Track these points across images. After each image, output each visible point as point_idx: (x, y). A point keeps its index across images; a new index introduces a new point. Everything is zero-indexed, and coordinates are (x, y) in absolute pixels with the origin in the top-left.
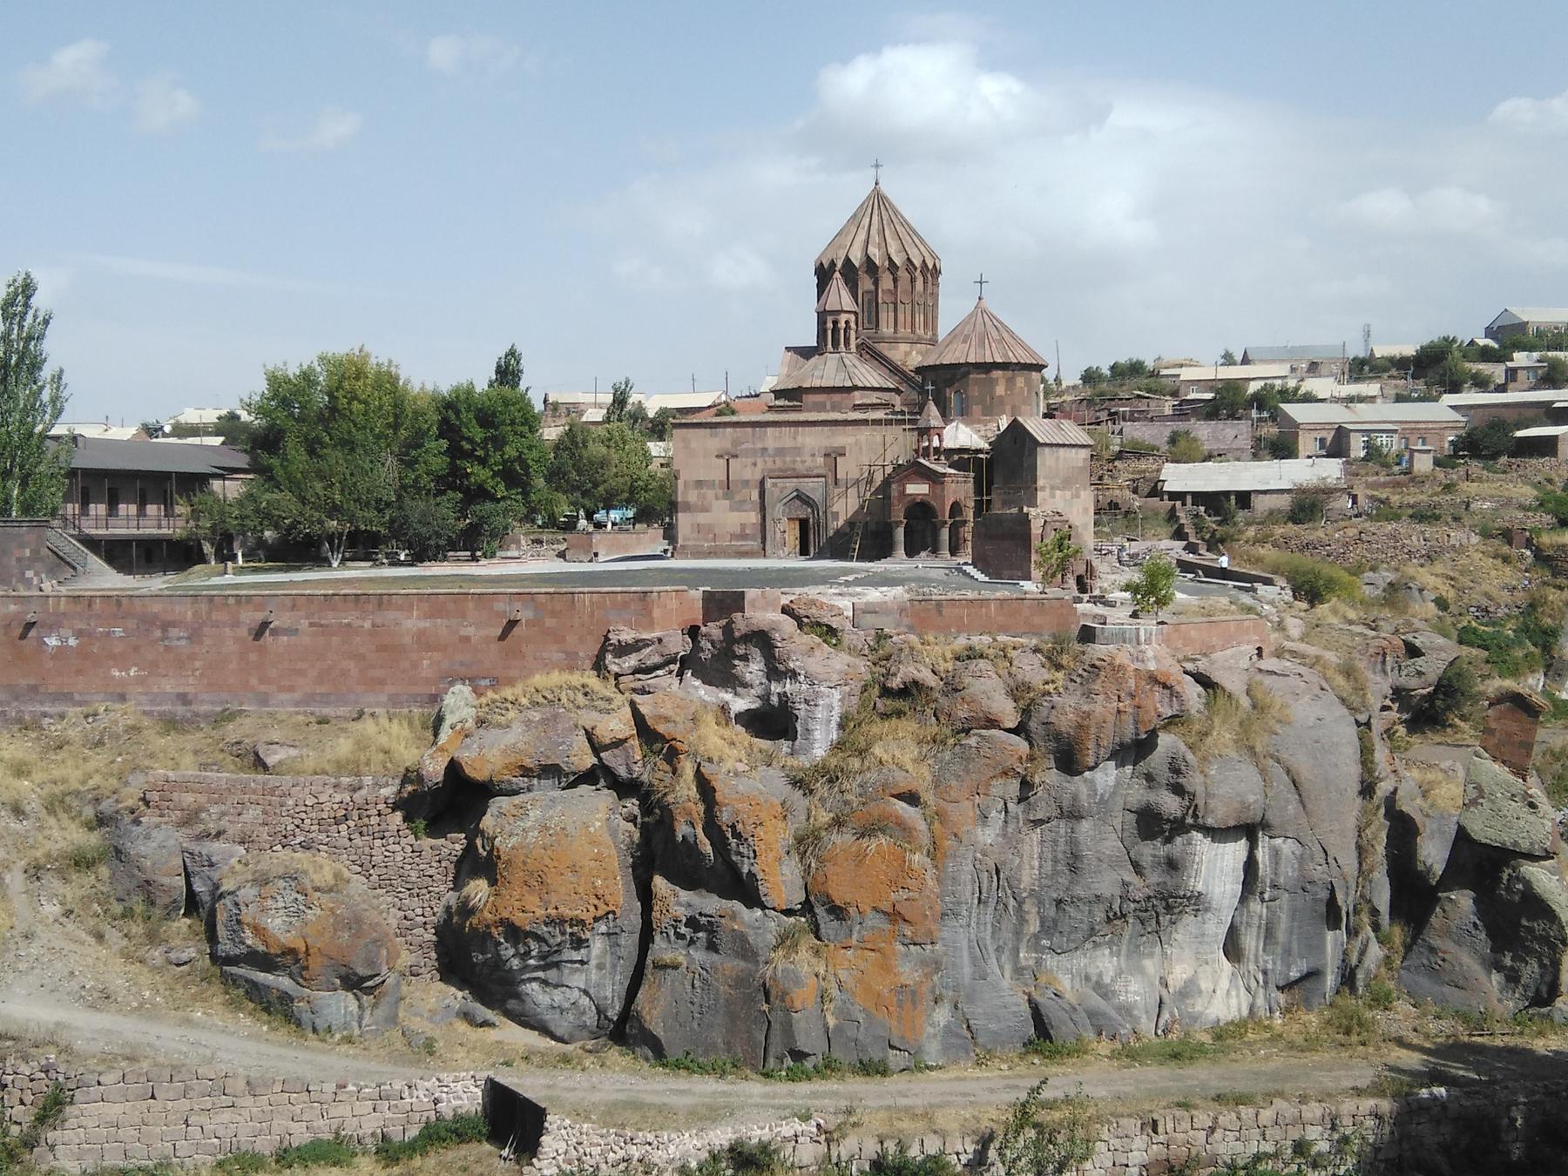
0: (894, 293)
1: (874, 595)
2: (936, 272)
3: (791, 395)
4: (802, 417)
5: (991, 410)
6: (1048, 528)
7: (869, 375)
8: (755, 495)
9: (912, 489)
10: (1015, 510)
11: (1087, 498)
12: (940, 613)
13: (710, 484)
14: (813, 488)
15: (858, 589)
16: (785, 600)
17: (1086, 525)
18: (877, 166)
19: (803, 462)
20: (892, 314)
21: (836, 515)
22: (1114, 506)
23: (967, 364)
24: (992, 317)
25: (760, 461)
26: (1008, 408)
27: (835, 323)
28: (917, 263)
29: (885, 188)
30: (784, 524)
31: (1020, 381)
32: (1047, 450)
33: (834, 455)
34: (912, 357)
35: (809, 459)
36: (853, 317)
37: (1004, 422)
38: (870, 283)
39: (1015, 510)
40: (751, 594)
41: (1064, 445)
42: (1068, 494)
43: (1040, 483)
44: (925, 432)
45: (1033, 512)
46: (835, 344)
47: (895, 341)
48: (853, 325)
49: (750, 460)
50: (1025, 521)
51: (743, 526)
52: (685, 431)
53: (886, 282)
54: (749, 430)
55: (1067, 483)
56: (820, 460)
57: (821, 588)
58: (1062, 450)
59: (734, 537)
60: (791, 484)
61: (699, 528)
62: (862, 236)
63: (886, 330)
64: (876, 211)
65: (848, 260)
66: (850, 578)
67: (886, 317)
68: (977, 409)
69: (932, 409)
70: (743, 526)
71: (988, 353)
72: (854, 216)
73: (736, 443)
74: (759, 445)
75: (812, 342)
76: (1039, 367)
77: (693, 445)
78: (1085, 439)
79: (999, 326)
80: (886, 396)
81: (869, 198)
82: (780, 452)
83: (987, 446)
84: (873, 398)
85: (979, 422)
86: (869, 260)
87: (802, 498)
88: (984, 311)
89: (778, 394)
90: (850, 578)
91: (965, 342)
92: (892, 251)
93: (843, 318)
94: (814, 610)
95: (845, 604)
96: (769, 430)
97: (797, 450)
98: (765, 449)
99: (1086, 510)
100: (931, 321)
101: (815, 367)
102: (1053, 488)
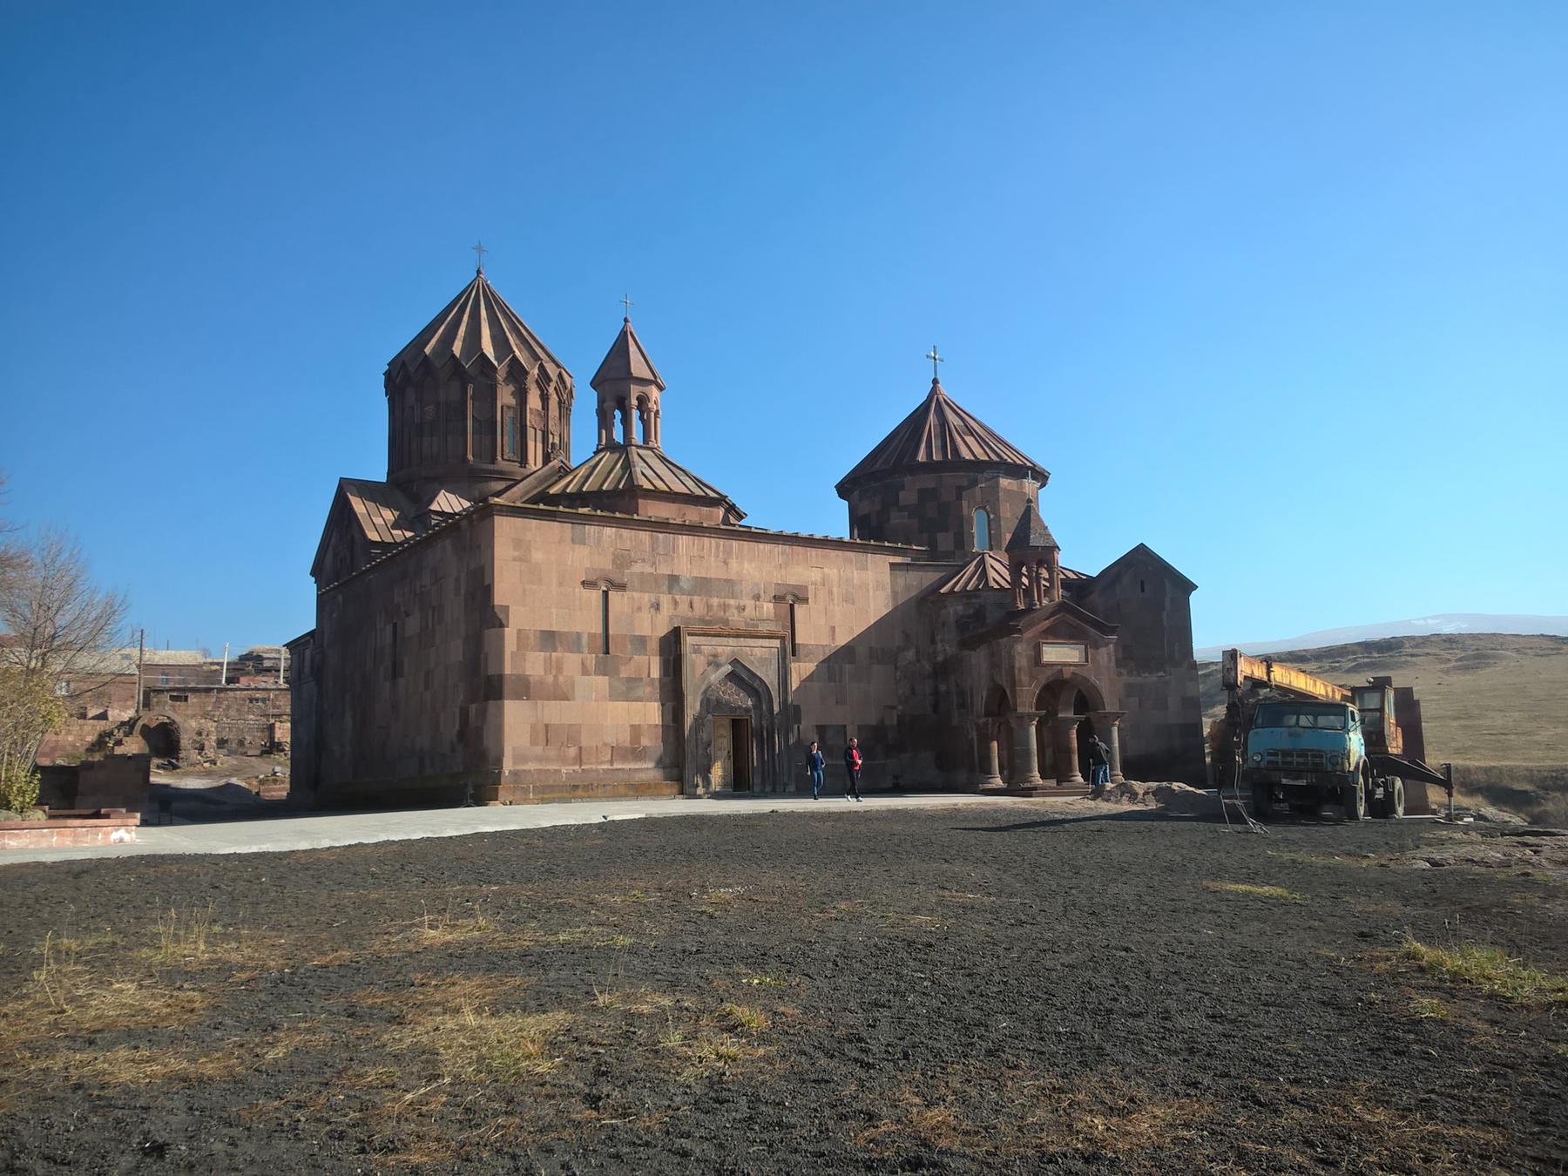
8: (656, 673)
13: (573, 642)
25: (665, 600)
33: (791, 600)
35: (749, 603)
49: (647, 598)
51: (636, 730)
56: (768, 608)
59: (617, 752)
60: (726, 648)
61: (547, 734)
70: (636, 730)
73: (622, 560)
74: (664, 570)
77: (537, 556)
82: (703, 585)
87: (740, 676)
96: (683, 541)
97: (730, 586)
98: (674, 579)
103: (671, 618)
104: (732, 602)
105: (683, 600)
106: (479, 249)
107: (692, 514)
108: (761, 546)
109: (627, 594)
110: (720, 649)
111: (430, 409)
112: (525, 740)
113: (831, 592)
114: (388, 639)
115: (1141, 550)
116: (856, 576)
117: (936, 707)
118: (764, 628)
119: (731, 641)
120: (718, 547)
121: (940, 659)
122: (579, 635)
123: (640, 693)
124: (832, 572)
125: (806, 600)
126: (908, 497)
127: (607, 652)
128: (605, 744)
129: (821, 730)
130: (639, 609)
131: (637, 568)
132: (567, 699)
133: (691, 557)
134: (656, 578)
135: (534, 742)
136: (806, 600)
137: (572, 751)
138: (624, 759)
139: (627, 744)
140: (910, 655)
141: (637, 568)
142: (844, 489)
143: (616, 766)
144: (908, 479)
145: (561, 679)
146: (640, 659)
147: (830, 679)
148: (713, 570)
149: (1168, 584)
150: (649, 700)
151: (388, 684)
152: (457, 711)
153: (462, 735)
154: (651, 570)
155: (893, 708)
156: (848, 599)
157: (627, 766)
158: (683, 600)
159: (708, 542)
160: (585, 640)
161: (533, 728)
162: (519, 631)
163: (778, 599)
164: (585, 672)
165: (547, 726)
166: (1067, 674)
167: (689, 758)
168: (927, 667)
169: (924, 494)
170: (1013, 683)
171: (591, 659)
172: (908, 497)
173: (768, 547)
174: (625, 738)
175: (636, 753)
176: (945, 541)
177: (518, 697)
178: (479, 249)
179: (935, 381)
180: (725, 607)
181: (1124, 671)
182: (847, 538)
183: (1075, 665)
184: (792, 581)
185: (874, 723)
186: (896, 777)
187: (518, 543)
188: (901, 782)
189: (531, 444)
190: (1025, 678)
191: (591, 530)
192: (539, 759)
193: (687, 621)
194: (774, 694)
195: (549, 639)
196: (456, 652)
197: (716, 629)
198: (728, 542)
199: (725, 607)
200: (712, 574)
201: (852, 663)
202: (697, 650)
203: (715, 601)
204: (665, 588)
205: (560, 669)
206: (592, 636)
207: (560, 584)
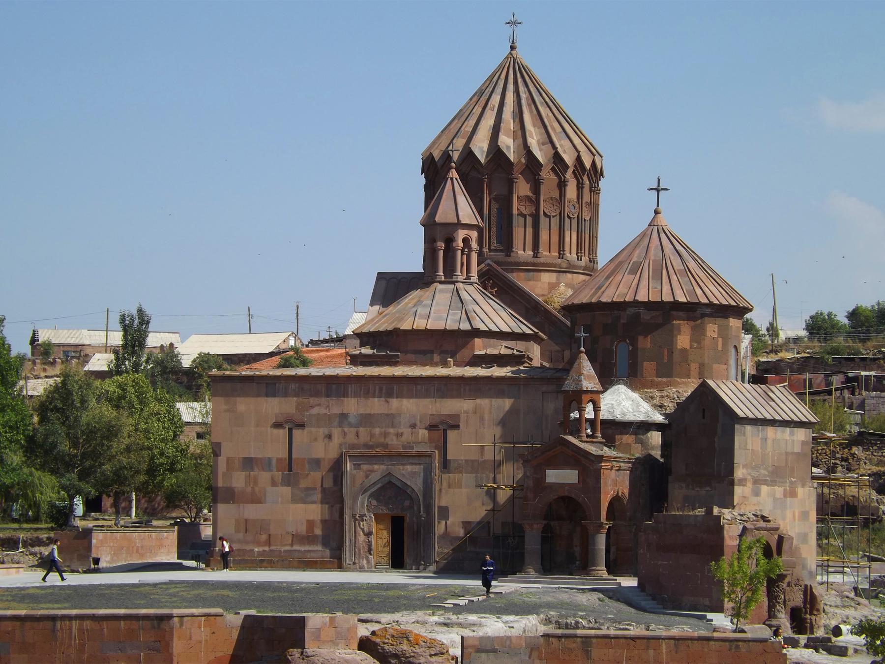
0: (534, 200)
1: (494, 626)
2: (596, 173)
3: (383, 343)
4: (399, 371)
5: (668, 370)
6: (748, 539)
7: (495, 316)
9: (553, 476)
10: (700, 512)
11: (806, 497)
12: (587, 653)
13: (265, 464)
14: (410, 474)
15: (473, 618)
16: (364, 631)
17: (804, 537)
18: (513, 23)
19: (399, 435)
20: (530, 231)
21: (444, 512)
22: (850, 509)
23: (636, 303)
24: (672, 238)
25: (336, 432)
26: (694, 367)
27: (450, 241)
28: (569, 158)
29: (524, 55)
30: (369, 523)
31: (712, 329)
32: (749, 428)
34: (555, 290)
35: (407, 431)
36: (474, 234)
37: (686, 389)
38: (501, 188)
39: (700, 512)
40: (315, 620)
41: (773, 423)
42: (779, 491)
43: (739, 473)
44: (576, 398)
45: (727, 514)
46: (450, 270)
47: (534, 268)
48: (474, 245)
49: (322, 431)
50: (716, 528)
51: (311, 524)
53: (522, 188)
55: (776, 475)
56: (423, 433)
57: (420, 615)
58: (770, 431)
59: (297, 538)
61: (246, 526)
62: (488, 121)
63: (523, 253)
64: (511, 87)
65: (468, 154)
66: (462, 602)
67: (521, 234)
68: (648, 367)
69: (586, 367)
71: (666, 288)
72: (480, 93)
74: (336, 410)
75: (416, 265)
76: (740, 311)
78: (803, 412)
79: (681, 248)
80: (519, 347)
81: (501, 67)
82: (367, 420)
83: (659, 418)
84: (501, 348)
85: (653, 385)
86: (496, 152)
88: (662, 231)
89: (364, 337)
90: (462, 602)
91: (633, 272)
92: (533, 142)
93: (461, 234)
94: (405, 647)
95: (451, 639)
97: (391, 419)
98: (343, 417)
99: (805, 515)
100: (588, 243)
101: (419, 302)
102: (757, 482)
103: (341, 445)
104: (392, 430)
108: (419, 387)
113: (482, 419)
118: (414, 451)
122: (270, 459)
127: (290, 470)
128: (288, 533)
130: (316, 439)
132: (259, 501)
134: (329, 418)
135: (237, 531)
136: (456, 427)
137: (264, 537)
139: (304, 533)
143: (296, 547)
145: (257, 489)
154: (323, 411)
157: (303, 548)
160: (274, 462)
161: (237, 521)
162: (228, 459)
163: (432, 427)
164: (274, 484)
165: (246, 520)
171: (278, 475)
174: (303, 529)
175: (309, 539)
177: (226, 501)
179: (656, 212)
180: (386, 435)
181: (684, 485)
193: (353, 446)
194: (421, 499)
195: (249, 463)
199: (386, 435)
203: (377, 431)
204: (336, 423)
205: (256, 483)
206: (279, 460)
207: (257, 426)
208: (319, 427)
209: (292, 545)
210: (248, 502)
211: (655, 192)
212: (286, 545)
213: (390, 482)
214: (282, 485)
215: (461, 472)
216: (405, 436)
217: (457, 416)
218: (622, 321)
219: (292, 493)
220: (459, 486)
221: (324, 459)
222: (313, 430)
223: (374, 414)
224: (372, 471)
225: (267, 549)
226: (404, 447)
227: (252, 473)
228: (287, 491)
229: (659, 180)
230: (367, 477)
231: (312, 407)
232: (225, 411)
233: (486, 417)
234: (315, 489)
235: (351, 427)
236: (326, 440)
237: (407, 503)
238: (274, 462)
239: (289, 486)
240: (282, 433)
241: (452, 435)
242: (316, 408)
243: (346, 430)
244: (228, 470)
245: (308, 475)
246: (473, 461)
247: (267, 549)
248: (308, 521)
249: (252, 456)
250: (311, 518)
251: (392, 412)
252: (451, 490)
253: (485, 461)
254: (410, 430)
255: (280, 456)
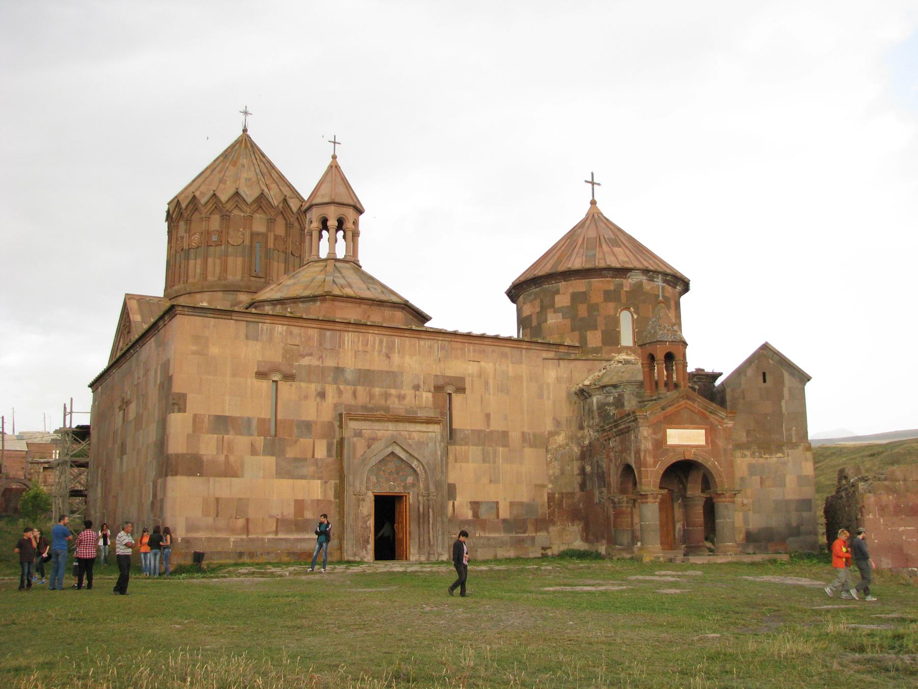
8: (321, 451)
19: (401, 397)
25: (330, 390)
33: (447, 390)
35: (408, 392)
49: (313, 388)
51: (300, 505)
52: (198, 321)
54: (314, 333)
56: (427, 397)
59: (282, 523)
60: (387, 430)
70: (300, 505)
73: (290, 354)
74: (330, 363)
77: (214, 350)
82: (366, 377)
96: (349, 338)
97: (393, 377)
103: (335, 406)
104: (393, 391)
105: (348, 390)
106: (246, 113)
107: (376, 316)
108: (422, 343)
109: (295, 384)
110: (380, 434)
111: (196, 237)
112: (196, 513)
113: (487, 383)
114: (120, 423)
115: (766, 347)
116: (511, 369)
117: (583, 486)
119: (391, 426)
120: (381, 342)
121: (587, 442)
122: (249, 420)
123: (304, 471)
124: (488, 366)
125: (461, 390)
126: (563, 300)
128: (271, 517)
129: (475, 505)
130: (306, 397)
131: (306, 361)
132: (235, 475)
133: (355, 352)
135: (205, 513)
136: (461, 390)
137: (241, 522)
138: (289, 531)
140: (560, 439)
141: (306, 361)
142: (515, 292)
144: (562, 285)
145: (232, 458)
146: (306, 442)
147: (484, 460)
148: (377, 363)
149: (786, 375)
150: (313, 477)
151: (118, 460)
152: (151, 484)
153: (153, 503)
154: (318, 363)
155: (544, 486)
156: (502, 389)
158: (348, 390)
159: (374, 339)
160: (254, 424)
162: (195, 416)
163: (438, 389)
164: (254, 452)
165: (217, 500)
166: (689, 456)
167: (348, 530)
168: (576, 450)
169: (577, 298)
170: (640, 463)
171: (260, 441)
172: (563, 300)
173: (428, 343)
175: (299, 525)
176: (594, 339)
177: (191, 473)
178: (246, 113)
181: (747, 453)
182: (515, 336)
183: (697, 447)
184: (450, 373)
185: (525, 500)
186: (543, 548)
187: (197, 339)
188: (549, 552)
189: (275, 264)
190: (650, 460)
191: (264, 327)
192: (208, 528)
193: (349, 408)
195: (222, 423)
196: (151, 434)
197: (370, 414)
198: (390, 339)
199: (387, 396)
200: (376, 367)
201: (506, 445)
202: (359, 434)
203: (377, 391)
204: (330, 379)
205: (230, 450)
206: (262, 421)
207: (234, 375)
208: (310, 381)
209: (276, 533)
210: (220, 476)
211: (590, 185)
212: (268, 533)
213: (392, 453)
214: (265, 454)
215: (467, 444)
216: (408, 398)
217: (462, 379)
218: (625, 289)
219: (277, 465)
220: (466, 460)
221: (315, 423)
222: (303, 385)
223: (373, 371)
224: (374, 439)
225: (244, 537)
226: (406, 410)
227: (226, 437)
228: (270, 461)
229: (592, 174)
230: (369, 447)
231: (304, 356)
232: (194, 353)
233: (491, 381)
234: (305, 459)
235: (348, 384)
236: (318, 399)
237: (410, 479)
238: (254, 424)
239: (272, 455)
240: (265, 385)
241: (457, 399)
242: (307, 358)
243: (342, 387)
244: (194, 431)
245: (296, 442)
246: (479, 432)
247: (244, 537)
248: (296, 501)
249: (227, 414)
250: (300, 497)
251: (395, 369)
252: (458, 465)
253: (491, 432)
254: (413, 391)
255: (263, 416)
